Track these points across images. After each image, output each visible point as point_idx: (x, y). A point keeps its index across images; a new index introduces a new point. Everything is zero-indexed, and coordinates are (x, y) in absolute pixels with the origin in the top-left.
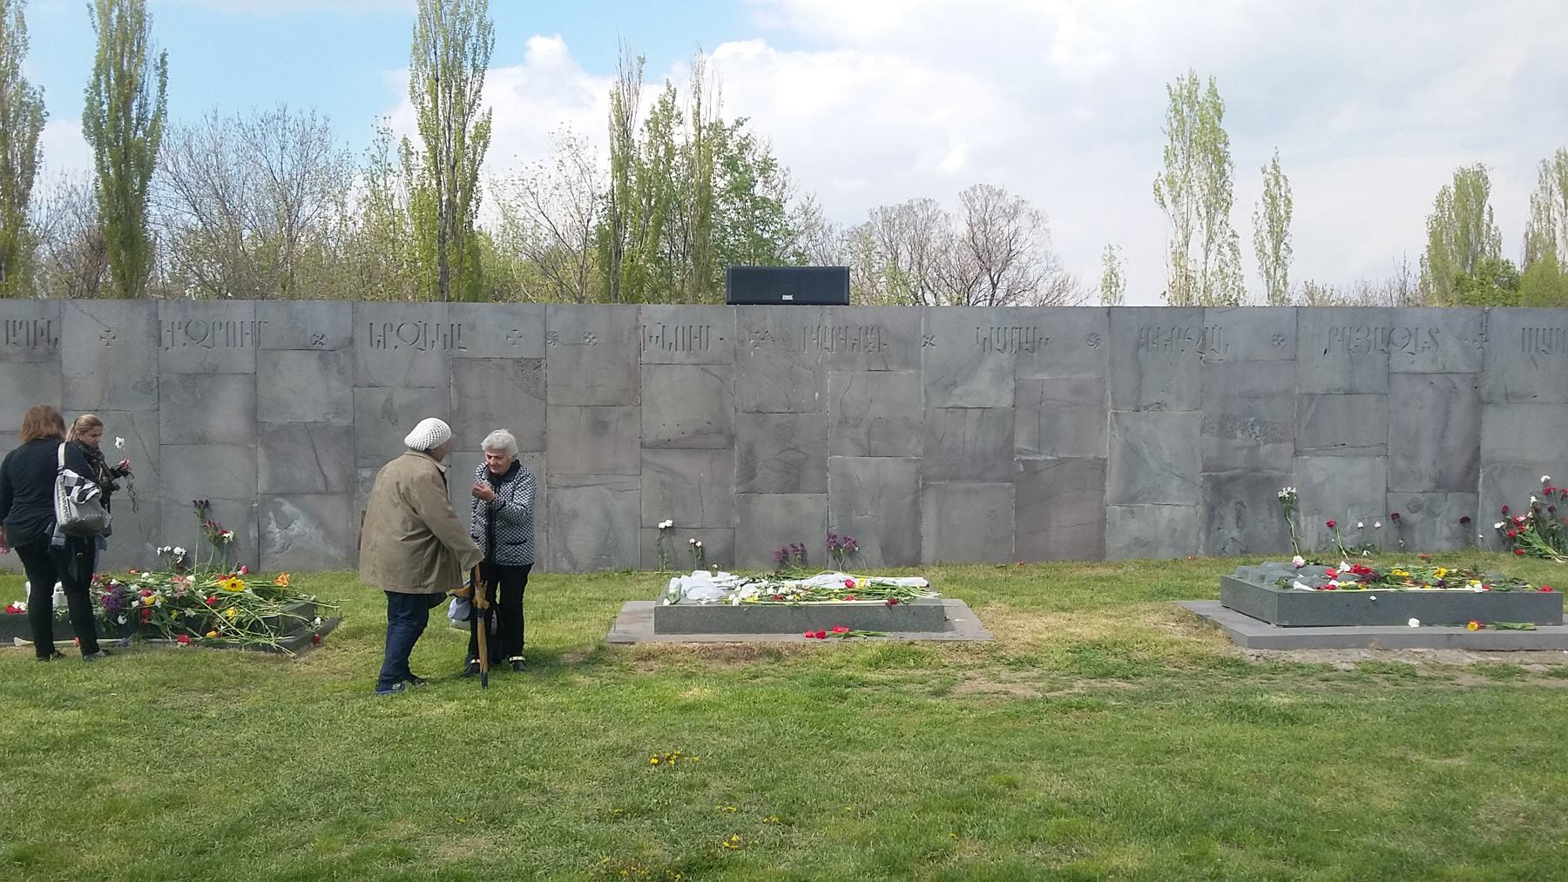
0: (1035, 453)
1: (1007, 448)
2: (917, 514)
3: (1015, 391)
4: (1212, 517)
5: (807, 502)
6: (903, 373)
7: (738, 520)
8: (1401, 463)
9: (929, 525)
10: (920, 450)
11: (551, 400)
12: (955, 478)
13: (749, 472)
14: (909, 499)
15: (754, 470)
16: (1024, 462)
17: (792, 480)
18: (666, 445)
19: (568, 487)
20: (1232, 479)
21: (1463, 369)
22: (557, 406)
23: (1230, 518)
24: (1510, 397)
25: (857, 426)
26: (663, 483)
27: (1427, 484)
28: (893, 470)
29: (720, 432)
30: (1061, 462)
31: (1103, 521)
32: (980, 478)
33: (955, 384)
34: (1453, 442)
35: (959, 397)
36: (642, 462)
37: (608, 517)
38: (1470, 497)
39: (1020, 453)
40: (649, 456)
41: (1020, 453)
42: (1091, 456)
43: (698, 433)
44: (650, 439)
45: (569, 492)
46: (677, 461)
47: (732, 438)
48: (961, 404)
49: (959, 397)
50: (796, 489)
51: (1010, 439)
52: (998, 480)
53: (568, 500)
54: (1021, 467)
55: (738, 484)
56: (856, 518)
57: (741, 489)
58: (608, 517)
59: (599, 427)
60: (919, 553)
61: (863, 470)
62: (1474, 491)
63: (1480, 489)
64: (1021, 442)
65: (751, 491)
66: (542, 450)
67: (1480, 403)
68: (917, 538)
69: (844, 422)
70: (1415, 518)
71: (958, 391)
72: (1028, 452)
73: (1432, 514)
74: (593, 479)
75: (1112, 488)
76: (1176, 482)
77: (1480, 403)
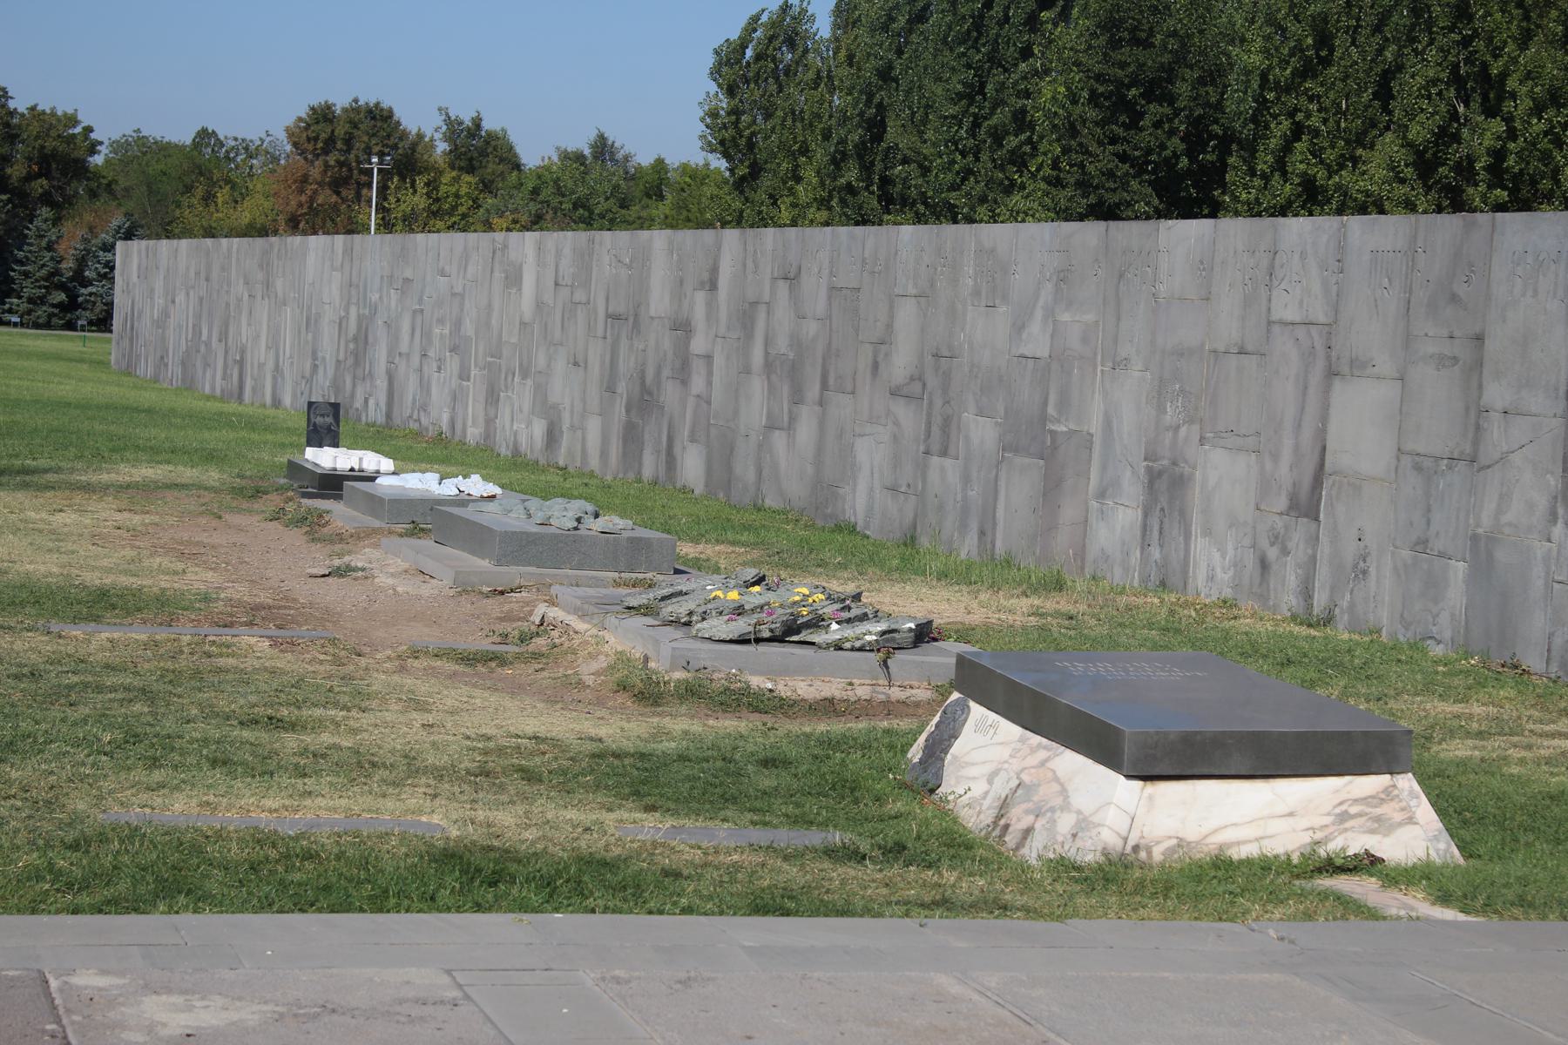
4: (1145, 528)
8: (1269, 465)
20: (1160, 474)
21: (1322, 319)
23: (1156, 533)
24: (1359, 366)
27: (1282, 503)
34: (1307, 433)
38: (1314, 525)
51: (1045, 403)
62: (1317, 519)
63: (1322, 516)
64: (1051, 410)
67: (1332, 373)
70: (1273, 553)
73: (1285, 552)
76: (1128, 473)
77: (1332, 373)
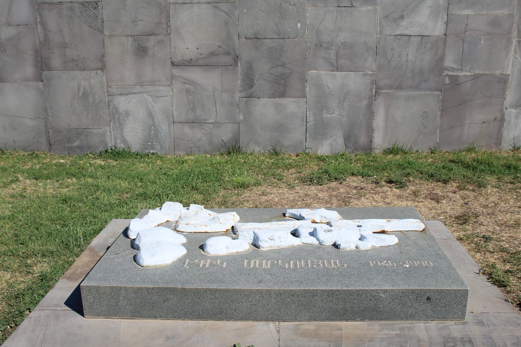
0: (458, 70)
1: (438, 66)
2: (371, 113)
3: (447, 24)
5: (291, 104)
6: (364, 8)
7: (241, 117)
9: (379, 121)
10: (374, 67)
11: (106, 32)
12: (400, 87)
13: (249, 82)
14: (365, 103)
15: (252, 80)
16: (450, 77)
17: (281, 88)
18: (188, 64)
19: (121, 94)
22: (111, 36)
25: (328, 48)
26: (188, 91)
28: (355, 82)
29: (228, 53)
30: (476, 77)
31: (502, 120)
32: (417, 88)
33: (402, 17)
35: (407, 27)
36: (173, 77)
37: (151, 115)
39: (447, 69)
40: (176, 71)
41: (447, 69)
42: (498, 72)
43: (212, 54)
44: (177, 59)
45: (122, 99)
46: (195, 75)
47: (236, 58)
48: (406, 32)
49: (407, 27)
50: (283, 95)
51: (441, 59)
52: (430, 90)
53: (123, 103)
54: (447, 81)
55: (241, 92)
56: (326, 116)
57: (243, 94)
58: (151, 115)
59: (141, 51)
60: (371, 142)
61: (332, 80)
64: (448, 62)
65: (251, 96)
66: (103, 68)
68: (370, 131)
69: (319, 45)
71: (404, 23)
72: (453, 69)
74: (138, 89)
75: (510, 97)
